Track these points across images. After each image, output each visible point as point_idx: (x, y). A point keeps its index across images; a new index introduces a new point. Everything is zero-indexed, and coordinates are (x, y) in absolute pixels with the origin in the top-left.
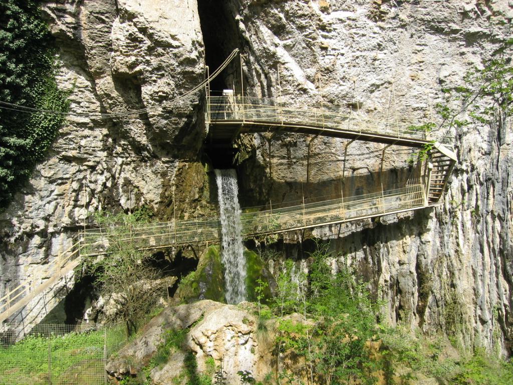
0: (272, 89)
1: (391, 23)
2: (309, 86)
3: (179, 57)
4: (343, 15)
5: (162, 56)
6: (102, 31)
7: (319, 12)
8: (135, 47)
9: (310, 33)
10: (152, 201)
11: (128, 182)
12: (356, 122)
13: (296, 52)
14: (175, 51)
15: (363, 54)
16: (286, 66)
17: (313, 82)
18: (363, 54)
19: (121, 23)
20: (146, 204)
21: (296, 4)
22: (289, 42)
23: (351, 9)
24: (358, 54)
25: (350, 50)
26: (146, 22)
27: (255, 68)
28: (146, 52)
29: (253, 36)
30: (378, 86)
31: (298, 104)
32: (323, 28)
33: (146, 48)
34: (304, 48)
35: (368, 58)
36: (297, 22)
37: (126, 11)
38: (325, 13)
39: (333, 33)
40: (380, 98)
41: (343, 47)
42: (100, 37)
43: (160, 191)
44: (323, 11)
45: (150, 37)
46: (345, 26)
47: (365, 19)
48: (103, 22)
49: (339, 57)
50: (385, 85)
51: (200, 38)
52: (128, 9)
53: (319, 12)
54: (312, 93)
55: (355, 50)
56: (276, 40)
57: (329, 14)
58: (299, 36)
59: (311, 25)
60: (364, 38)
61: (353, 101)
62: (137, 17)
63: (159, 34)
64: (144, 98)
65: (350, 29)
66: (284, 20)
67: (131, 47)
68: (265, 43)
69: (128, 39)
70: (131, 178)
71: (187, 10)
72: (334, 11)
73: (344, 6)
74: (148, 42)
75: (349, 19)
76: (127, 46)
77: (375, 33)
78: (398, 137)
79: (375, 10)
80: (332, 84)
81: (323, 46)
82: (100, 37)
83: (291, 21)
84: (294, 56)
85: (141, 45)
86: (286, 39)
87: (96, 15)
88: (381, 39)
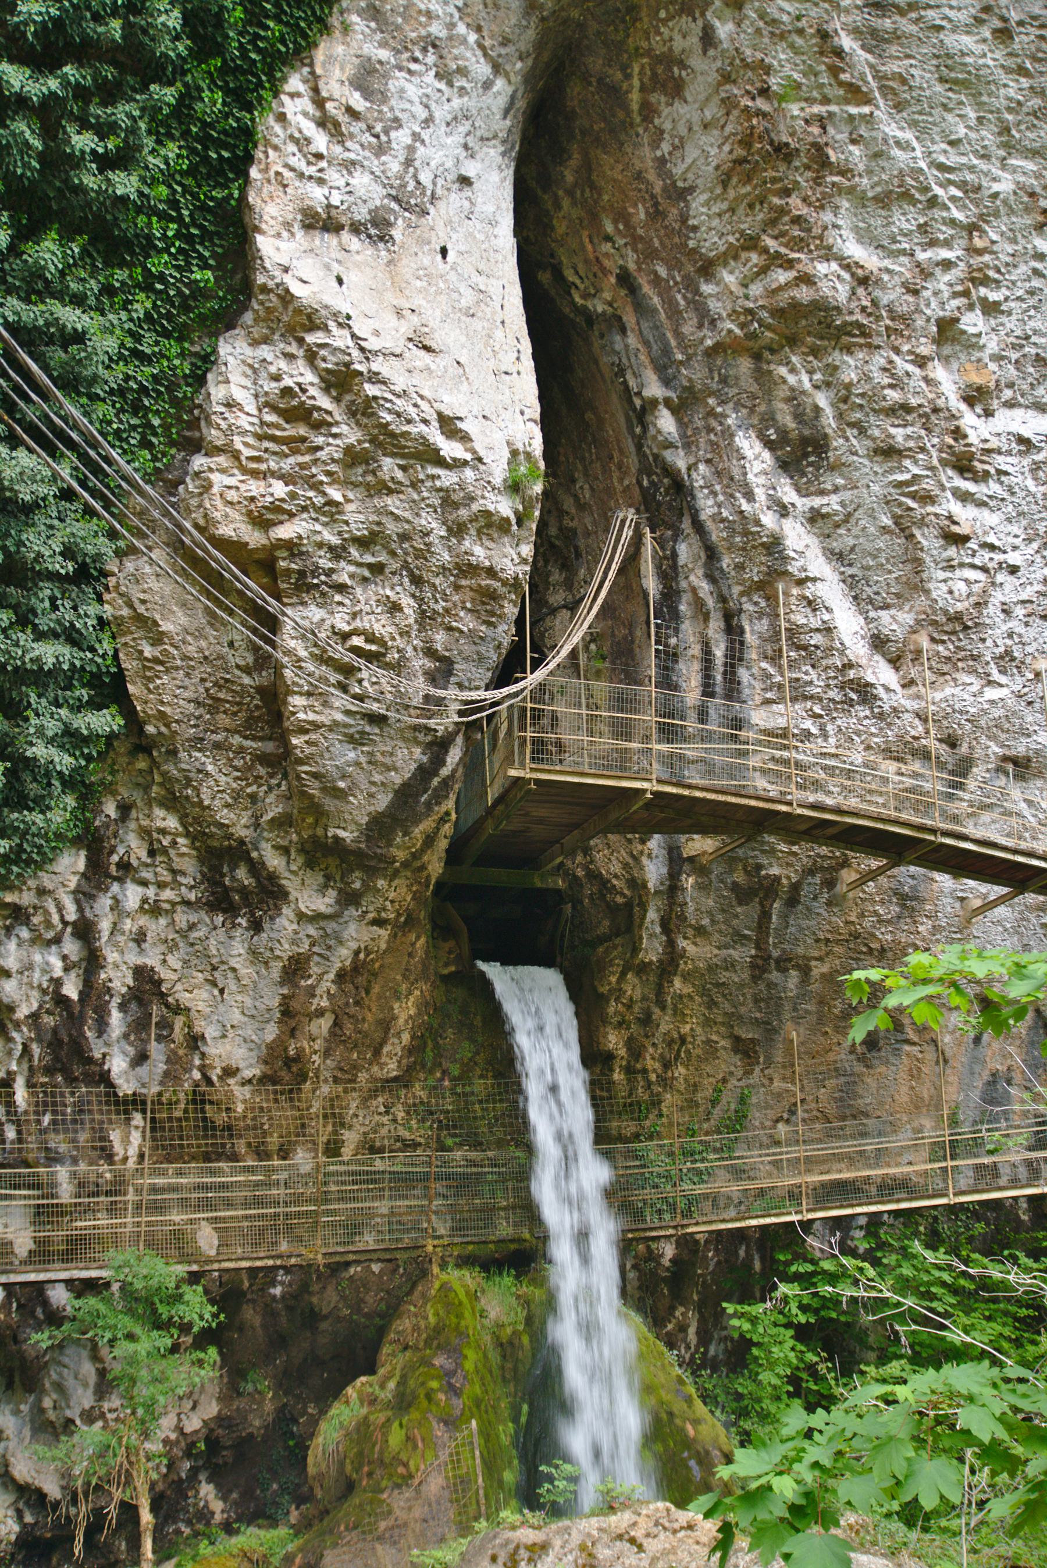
0: (743, 674)
2: (881, 674)
3: (456, 505)
5: (391, 492)
7: (957, 404)
8: (295, 444)
9: (916, 478)
10: (229, 1072)
11: (147, 986)
13: (851, 542)
14: (448, 478)
17: (895, 662)
20: (209, 1082)
22: (832, 503)
26: (355, 353)
27: (694, 590)
28: (333, 467)
29: (702, 467)
31: (832, 741)
32: (963, 465)
34: (885, 530)
36: (876, 433)
37: (287, 297)
38: (979, 410)
41: (1017, 542)
43: (271, 1032)
44: (969, 401)
45: (363, 411)
53: (957, 404)
56: (788, 494)
58: (875, 482)
59: (923, 449)
61: (1020, 747)
62: (326, 329)
64: (288, 653)
66: (829, 420)
67: (273, 439)
68: (750, 496)
69: (274, 409)
70: (164, 974)
71: (499, 334)
72: (1010, 405)
74: (350, 434)
76: (260, 438)
81: (955, 529)
83: (852, 425)
85: (320, 440)
86: (822, 493)
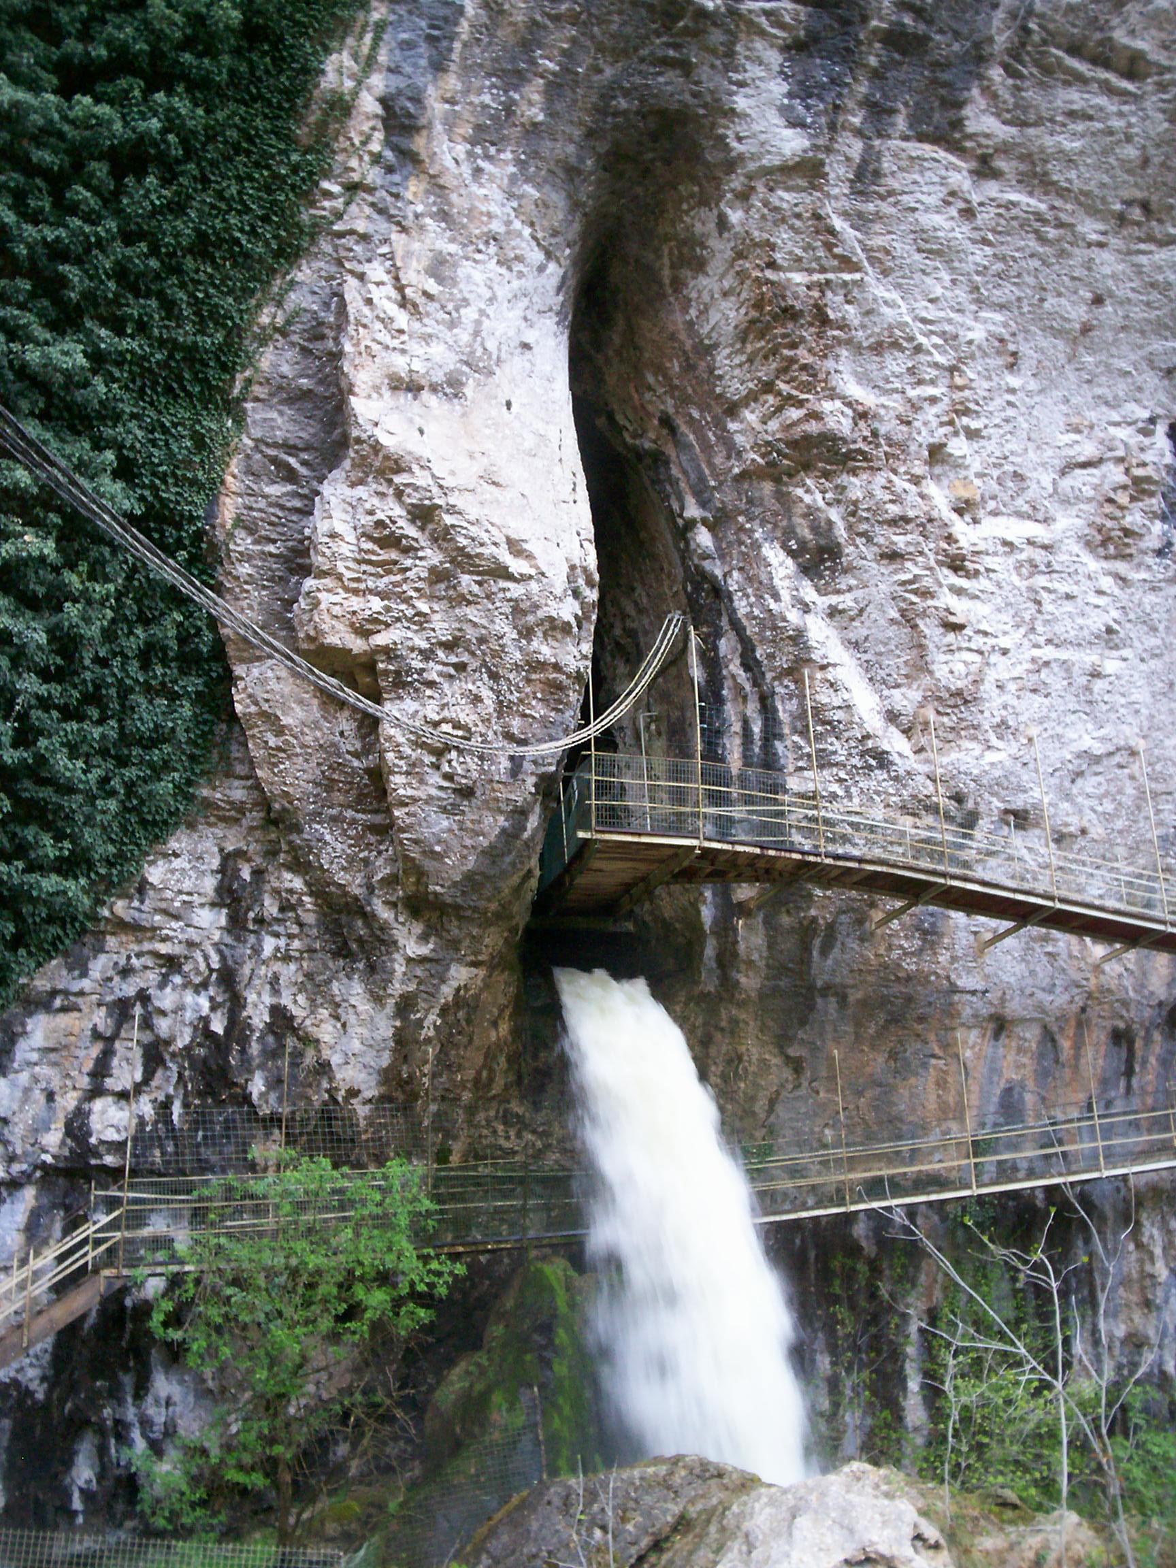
0: (779, 746)
1: (1149, 567)
2: (895, 743)
3: (524, 613)
4: (1018, 530)
5: (469, 603)
6: (282, 507)
7: (949, 515)
8: (388, 567)
9: (916, 578)
10: (353, 1093)
11: (281, 1019)
12: (1015, 863)
13: (865, 632)
14: (516, 590)
15: (1063, 654)
16: (831, 674)
17: (907, 732)
18: (1063, 654)
19: (353, 485)
20: (336, 1102)
21: (883, 482)
22: (846, 601)
23: (1040, 516)
24: (1048, 653)
25: (1026, 642)
26: (435, 490)
27: (733, 677)
28: (420, 585)
29: (735, 574)
30: (1097, 759)
31: (856, 800)
32: (956, 564)
33: (424, 575)
34: (893, 621)
35: (1076, 670)
36: (881, 540)
37: (377, 447)
38: (967, 518)
39: (983, 583)
40: (1100, 798)
41: (1007, 628)
42: (271, 524)
43: (386, 1060)
44: (960, 511)
45: (443, 537)
46: (1019, 566)
47: (1077, 548)
48: (291, 476)
49: (995, 658)
50: (1117, 759)
51: (592, 560)
52: (384, 440)
53: (949, 515)
54: (901, 766)
55: (1041, 640)
56: (809, 592)
57: (975, 521)
58: (881, 583)
59: (921, 553)
60: (1069, 607)
61: (1018, 802)
62: (410, 470)
63: (474, 531)
64: (390, 738)
65: (1031, 575)
66: (841, 532)
67: (370, 562)
68: (776, 597)
69: (370, 538)
70: (296, 1011)
71: (557, 470)
72: (995, 513)
73: (1020, 502)
74: (433, 557)
75: (1030, 542)
76: (359, 562)
77: (1100, 592)
78: (1164, 922)
79: (1109, 524)
80: (966, 744)
81: (952, 619)
82: (271, 524)
83: (860, 535)
84: (856, 645)
85: (408, 562)
86: (838, 592)
87: (271, 452)
88: (1115, 614)
